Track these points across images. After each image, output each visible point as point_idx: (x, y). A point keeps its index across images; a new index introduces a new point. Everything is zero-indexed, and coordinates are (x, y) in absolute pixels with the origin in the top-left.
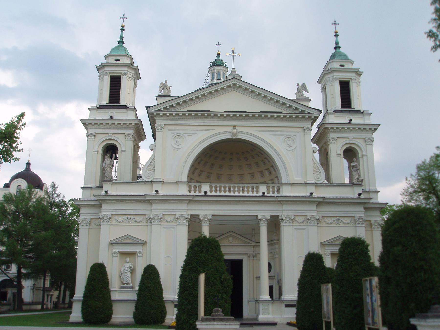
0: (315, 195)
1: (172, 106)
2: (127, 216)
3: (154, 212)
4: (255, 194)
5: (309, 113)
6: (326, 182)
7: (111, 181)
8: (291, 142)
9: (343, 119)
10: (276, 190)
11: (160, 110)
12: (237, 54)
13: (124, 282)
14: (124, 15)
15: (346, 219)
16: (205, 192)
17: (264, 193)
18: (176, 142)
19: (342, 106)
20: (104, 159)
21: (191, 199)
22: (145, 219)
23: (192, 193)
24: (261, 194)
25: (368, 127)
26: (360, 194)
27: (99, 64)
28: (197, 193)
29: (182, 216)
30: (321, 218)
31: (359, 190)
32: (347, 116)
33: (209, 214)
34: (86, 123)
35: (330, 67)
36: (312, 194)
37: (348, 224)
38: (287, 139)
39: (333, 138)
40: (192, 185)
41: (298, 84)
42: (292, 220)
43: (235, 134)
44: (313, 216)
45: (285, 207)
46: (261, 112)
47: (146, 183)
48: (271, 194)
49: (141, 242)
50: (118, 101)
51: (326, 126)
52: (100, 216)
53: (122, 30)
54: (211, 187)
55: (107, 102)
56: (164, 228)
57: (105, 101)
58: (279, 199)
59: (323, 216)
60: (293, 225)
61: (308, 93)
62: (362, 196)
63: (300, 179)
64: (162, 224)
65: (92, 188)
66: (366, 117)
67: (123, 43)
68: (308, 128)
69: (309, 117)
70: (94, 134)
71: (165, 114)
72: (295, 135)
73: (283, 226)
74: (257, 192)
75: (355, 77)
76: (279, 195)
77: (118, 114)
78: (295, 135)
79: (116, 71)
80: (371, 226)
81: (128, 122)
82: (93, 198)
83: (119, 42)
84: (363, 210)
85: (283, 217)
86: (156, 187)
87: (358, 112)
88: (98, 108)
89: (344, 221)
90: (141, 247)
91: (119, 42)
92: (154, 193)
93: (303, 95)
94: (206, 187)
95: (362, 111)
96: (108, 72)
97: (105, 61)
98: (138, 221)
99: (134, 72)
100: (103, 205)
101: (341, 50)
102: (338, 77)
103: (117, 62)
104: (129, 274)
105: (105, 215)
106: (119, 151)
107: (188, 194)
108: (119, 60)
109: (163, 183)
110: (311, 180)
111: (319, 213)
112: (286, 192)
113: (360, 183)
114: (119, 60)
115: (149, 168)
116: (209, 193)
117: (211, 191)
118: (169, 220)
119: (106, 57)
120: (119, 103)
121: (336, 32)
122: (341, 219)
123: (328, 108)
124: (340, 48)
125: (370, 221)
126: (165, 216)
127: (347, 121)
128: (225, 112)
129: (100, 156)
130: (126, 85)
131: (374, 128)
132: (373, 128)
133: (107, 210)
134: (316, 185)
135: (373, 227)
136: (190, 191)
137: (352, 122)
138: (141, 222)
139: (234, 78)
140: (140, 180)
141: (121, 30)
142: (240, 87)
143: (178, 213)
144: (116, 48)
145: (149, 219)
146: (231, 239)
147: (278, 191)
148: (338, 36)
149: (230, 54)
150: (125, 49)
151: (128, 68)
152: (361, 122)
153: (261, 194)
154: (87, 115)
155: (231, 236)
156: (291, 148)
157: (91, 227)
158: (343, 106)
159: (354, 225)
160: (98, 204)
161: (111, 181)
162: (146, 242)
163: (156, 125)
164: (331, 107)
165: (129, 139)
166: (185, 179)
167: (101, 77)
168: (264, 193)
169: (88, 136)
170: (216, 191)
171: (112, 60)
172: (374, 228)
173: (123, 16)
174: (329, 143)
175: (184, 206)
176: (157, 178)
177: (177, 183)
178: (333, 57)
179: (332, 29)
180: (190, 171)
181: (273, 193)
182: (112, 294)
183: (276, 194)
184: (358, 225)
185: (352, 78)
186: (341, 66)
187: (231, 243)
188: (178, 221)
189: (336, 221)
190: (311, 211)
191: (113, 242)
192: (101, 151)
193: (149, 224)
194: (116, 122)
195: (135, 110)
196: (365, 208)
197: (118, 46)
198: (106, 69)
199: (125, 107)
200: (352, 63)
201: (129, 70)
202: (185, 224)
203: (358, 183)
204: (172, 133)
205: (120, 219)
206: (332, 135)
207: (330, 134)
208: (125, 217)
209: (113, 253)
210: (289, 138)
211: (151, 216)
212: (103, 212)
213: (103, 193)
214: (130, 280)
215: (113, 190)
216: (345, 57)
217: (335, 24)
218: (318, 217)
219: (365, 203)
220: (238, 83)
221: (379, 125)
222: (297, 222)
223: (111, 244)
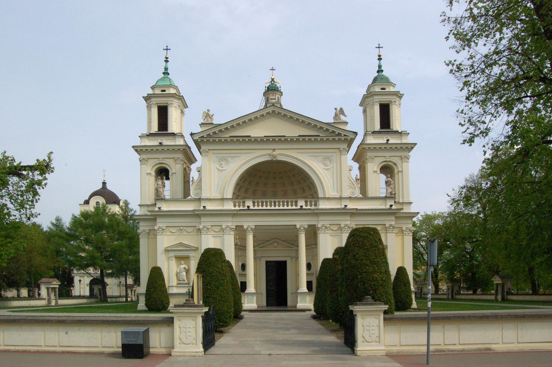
0: (348, 207)
4: (294, 207)
6: (361, 196)
7: (163, 200)
9: (381, 140)
10: (313, 203)
20: (156, 180)
23: (237, 208)
24: (299, 207)
25: (404, 146)
26: (391, 206)
28: (241, 208)
31: (390, 202)
34: (138, 149)
35: (372, 90)
36: (346, 206)
40: (237, 201)
45: (321, 218)
47: (194, 200)
48: (309, 207)
49: (193, 248)
50: (167, 130)
51: (364, 146)
52: (156, 228)
54: (254, 203)
55: (157, 130)
57: (155, 128)
62: (394, 207)
65: (148, 206)
66: (404, 137)
67: (169, 74)
74: (296, 205)
76: (316, 208)
77: (167, 142)
79: (162, 101)
81: (176, 148)
82: (149, 213)
83: (163, 73)
84: (394, 219)
86: (203, 204)
87: (396, 132)
88: (148, 135)
91: (163, 73)
92: (202, 208)
94: (249, 203)
95: (400, 131)
96: (155, 103)
97: (151, 92)
100: (157, 219)
101: (383, 73)
104: (184, 273)
105: (159, 228)
106: (170, 174)
107: (233, 208)
108: (164, 91)
110: (346, 194)
114: (164, 91)
116: (252, 207)
119: (153, 88)
120: (167, 130)
121: (379, 56)
123: (368, 130)
124: (382, 71)
126: (213, 227)
127: (385, 141)
128: (265, 137)
129: (153, 179)
130: (173, 114)
131: (410, 147)
132: (410, 146)
133: (161, 223)
134: (350, 198)
136: (235, 206)
137: (389, 142)
139: (273, 105)
140: (189, 198)
144: (161, 79)
147: (315, 205)
148: (381, 59)
150: (170, 79)
152: (399, 142)
154: (138, 142)
157: (150, 237)
158: (382, 127)
160: (153, 218)
161: (163, 200)
162: (198, 248)
164: (370, 129)
166: (229, 195)
167: (149, 107)
168: (301, 207)
169: (140, 161)
170: (258, 206)
171: (158, 91)
173: (166, 48)
175: (230, 219)
178: (375, 80)
180: (235, 189)
181: (311, 206)
183: (313, 207)
191: (169, 249)
192: (153, 173)
193: (199, 233)
194: (165, 148)
195: (182, 136)
196: (396, 218)
197: (163, 77)
198: (152, 100)
199: (173, 134)
200: (394, 85)
205: (173, 230)
206: (369, 154)
208: (178, 228)
209: (168, 258)
211: (201, 227)
212: (159, 225)
213: (157, 209)
214: (185, 277)
215: (165, 207)
216: (386, 80)
217: (379, 47)
219: (396, 213)
220: (277, 110)
221: (416, 144)
223: (167, 251)
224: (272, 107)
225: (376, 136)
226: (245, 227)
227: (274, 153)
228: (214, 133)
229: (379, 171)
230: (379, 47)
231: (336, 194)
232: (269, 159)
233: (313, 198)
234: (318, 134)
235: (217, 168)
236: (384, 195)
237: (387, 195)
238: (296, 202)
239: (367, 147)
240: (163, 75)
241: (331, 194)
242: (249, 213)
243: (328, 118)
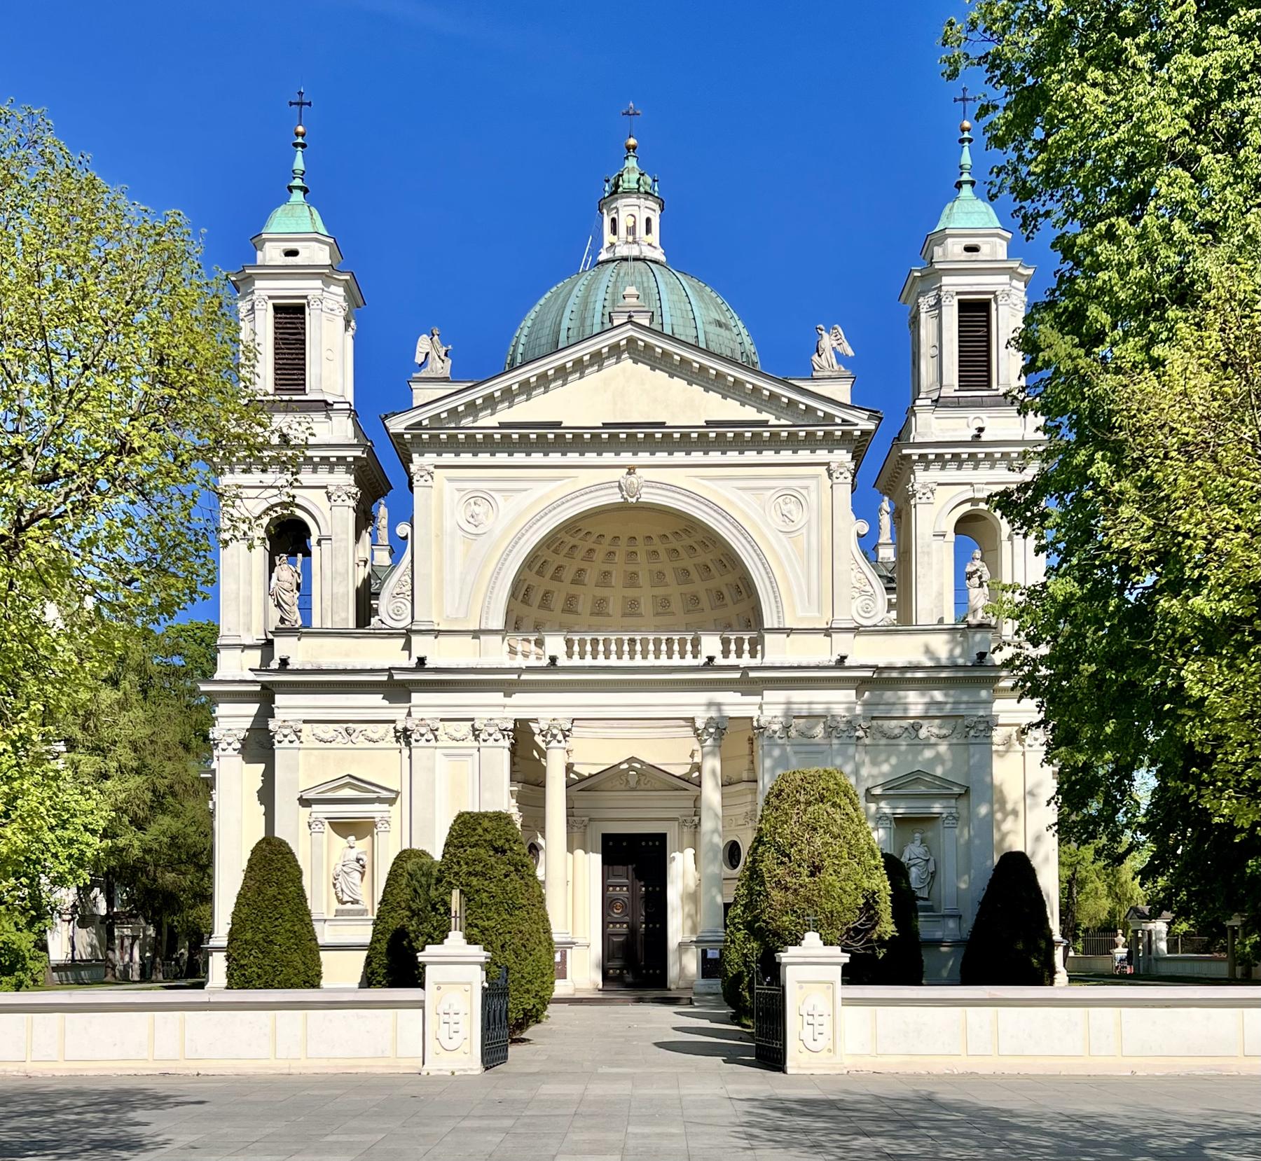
2: (345, 726)
4: (689, 661)
13: (346, 898)
16: (553, 659)
17: (711, 659)
21: (515, 677)
23: (520, 662)
32: (972, 416)
36: (845, 657)
47: (391, 634)
48: (732, 660)
51: (905, 452)
54: (569, 643)
64: (438, 744)
68: (841, 465)
72: (807, 488)
75: (1007, 287)
76: (756, 662)
78: (807, 488)
81: (333, 454)
90: (385, 807)
94: (555, 644)
96: (265, 293)
98: (375, 737)
103: (291, 260)
106: (313, 540)
107: (507, 662)
108: (294, 253)
109: (438, 633)
114: (294, 253)
115: (398, 590)
116: (562, 661)
117: (570, 655)
128: (606, 426)
129: (260, 555)
145: (405, 736)
153: (702, 660)
163: (413, 468)
166: (498, 622)
168: (711, 659)
173: (297, 100)
175: (497, 697)
177: (476, 634)
180: (513, 594)
181: (739, 655)
182: (317, 927)
183: (746, 661)
185: (999, 289)
186: (969, 249)
188: (482, 736)
199: (325, 407)
205: (327, 731)
206: (922, 478)
210: (787, 495)
224: (629, 326)
225: (942, 412)
227: (633, 479)
228: (453, 412)
229: (951, 536)
230: (964, 99)
232: (618, 499)
233: (748, 626)
234: (764, 416)
238: (696, 643)
239: (915, 453)
242: (550, 678)
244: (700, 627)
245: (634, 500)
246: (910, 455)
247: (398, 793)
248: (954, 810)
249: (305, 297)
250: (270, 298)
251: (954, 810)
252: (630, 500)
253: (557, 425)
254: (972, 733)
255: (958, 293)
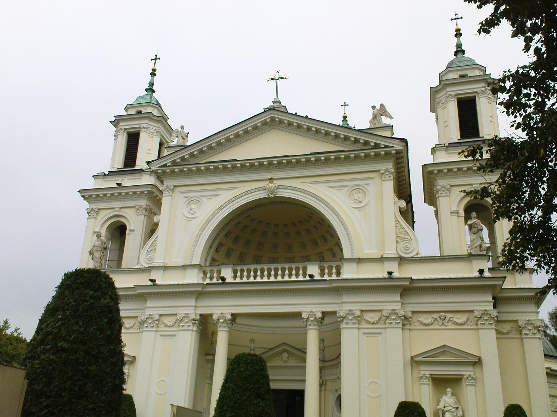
1: (183, 159)
3: (148, 312)
4: (301, 278)
5: (386, 147)
8: (360, 195)
11: (166, 164)
12: (282, 78)
14: (156, 56)
15: (459, 315)
18: (191, 210)
19: (461, 135)
21: (200, 289)
22: (138, 324)
27: (113, 119)
29: (187, 316)
30: (410, 315)
33: (227, 313)
37: (461, 324)
38: (353, 192)
39: (443, 187)
41: (374, 107)
42: (359, 319)
43: (272, 191)
44: (394, 312)
45: (346, 298)
46: (311, 154)
50: (134, 165)
51: (429, 169)
53: (153, 74)
54: (235, 272)
56: (161, 336)
58: (334, 285)
59: (413, 312)
60: (361, 326)
61: (391, 118)
63: (375, 251)
67: (154, 92)
69: (387, 154)
70: (96, 210)
71: (173, 172)
72: (367, 185)
73: (343, 328)
78: (367, 185)
79: (132, 125)
80: (521, 331)
81: (138, 190)
83: (146, 90)
85: (342, 314)
89: (455, 320)
91: (146, 90)
93: (380, 121)
94: (227, 273)
99: (159, 125)
102: (453, 93)
109: (165, 268)
110: (391, 252)
111: (405, 305)
112: (349, 272)
113: (484, 253)
115: (151, 248)
118: (168, 324)
122: (449, 315)
125: (516, 321)
135: (524, 332)
138: (132, 327)
141: (151, 74)
142: (290, 124)
143: (182, 312)
146: (285, 355)
147: (338, 273)
148: (461, 35)
149: (272, 79)
151: (149, 120)
155: (285, 351)
156: (360, 205)
158: (463, 136)
159: (474, 327)
165: (140, 213)
172: (527, 334)
174: (437, 196)
175: (192, 302)
176: (158, 261)
177: (184, 267)
179: (453, 26)
183: (334, 277)
184: (481, 327)
187: (285, 362)
189: (439, 319)
190: (392, 303)
201: (150, 123)
202: (191, 328)
203: (481, 253)
204: (185, 197)
206: (441, 183)
207: (438, 181)
210: (357, 189)
217: (455, 19)
218: (402, 313)
219: (493, 287)
222: (368, 322)
226: (215, 317)
231: (374, 253)
235: (186, 216)
236: (465, 253)
237: (473, 253)
238: (305, 269)
240: (146, 93)
241: (366, 252)
242: (223, 290)
243: (361, 120)
244: (307, 259)
245: (272, 196)
246: (433, 171)
247: (134, 357)
248: (472, 373)
249: (140, 128)
250: (125, 129)
251: (472, 373)
252: (271, 196)
253: (236, 160)
254: (480, 322)
255: (456, 95)
